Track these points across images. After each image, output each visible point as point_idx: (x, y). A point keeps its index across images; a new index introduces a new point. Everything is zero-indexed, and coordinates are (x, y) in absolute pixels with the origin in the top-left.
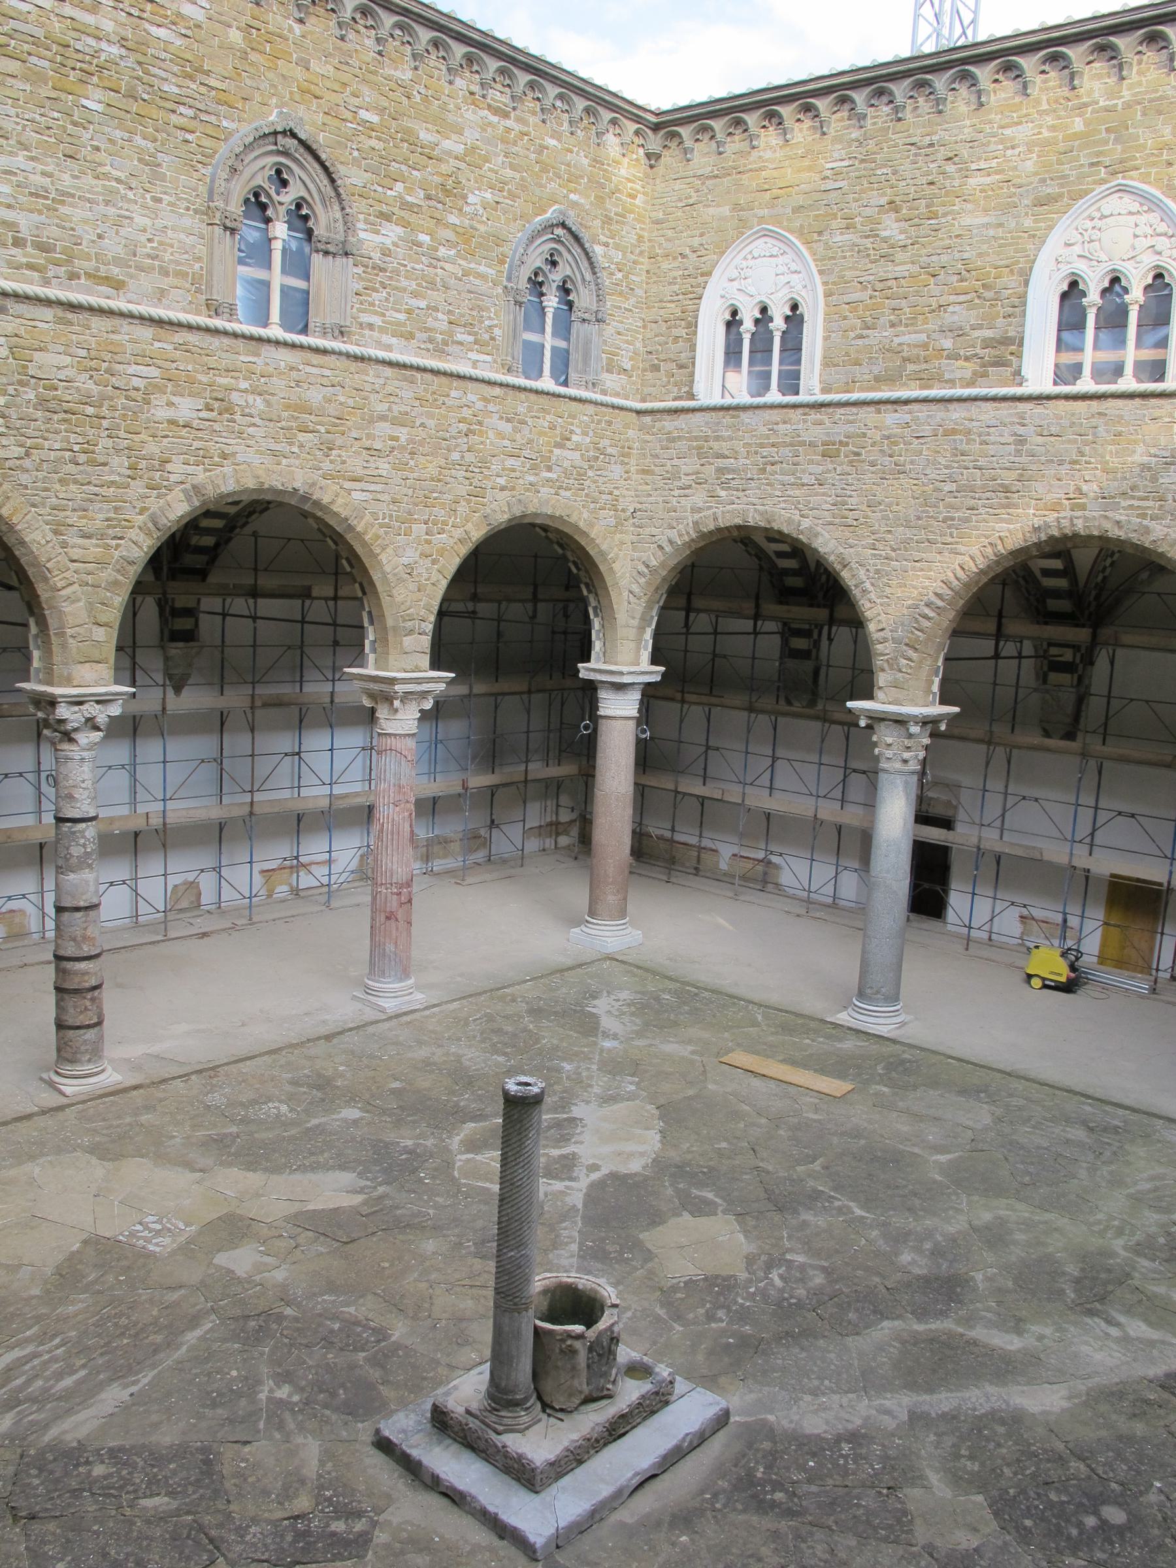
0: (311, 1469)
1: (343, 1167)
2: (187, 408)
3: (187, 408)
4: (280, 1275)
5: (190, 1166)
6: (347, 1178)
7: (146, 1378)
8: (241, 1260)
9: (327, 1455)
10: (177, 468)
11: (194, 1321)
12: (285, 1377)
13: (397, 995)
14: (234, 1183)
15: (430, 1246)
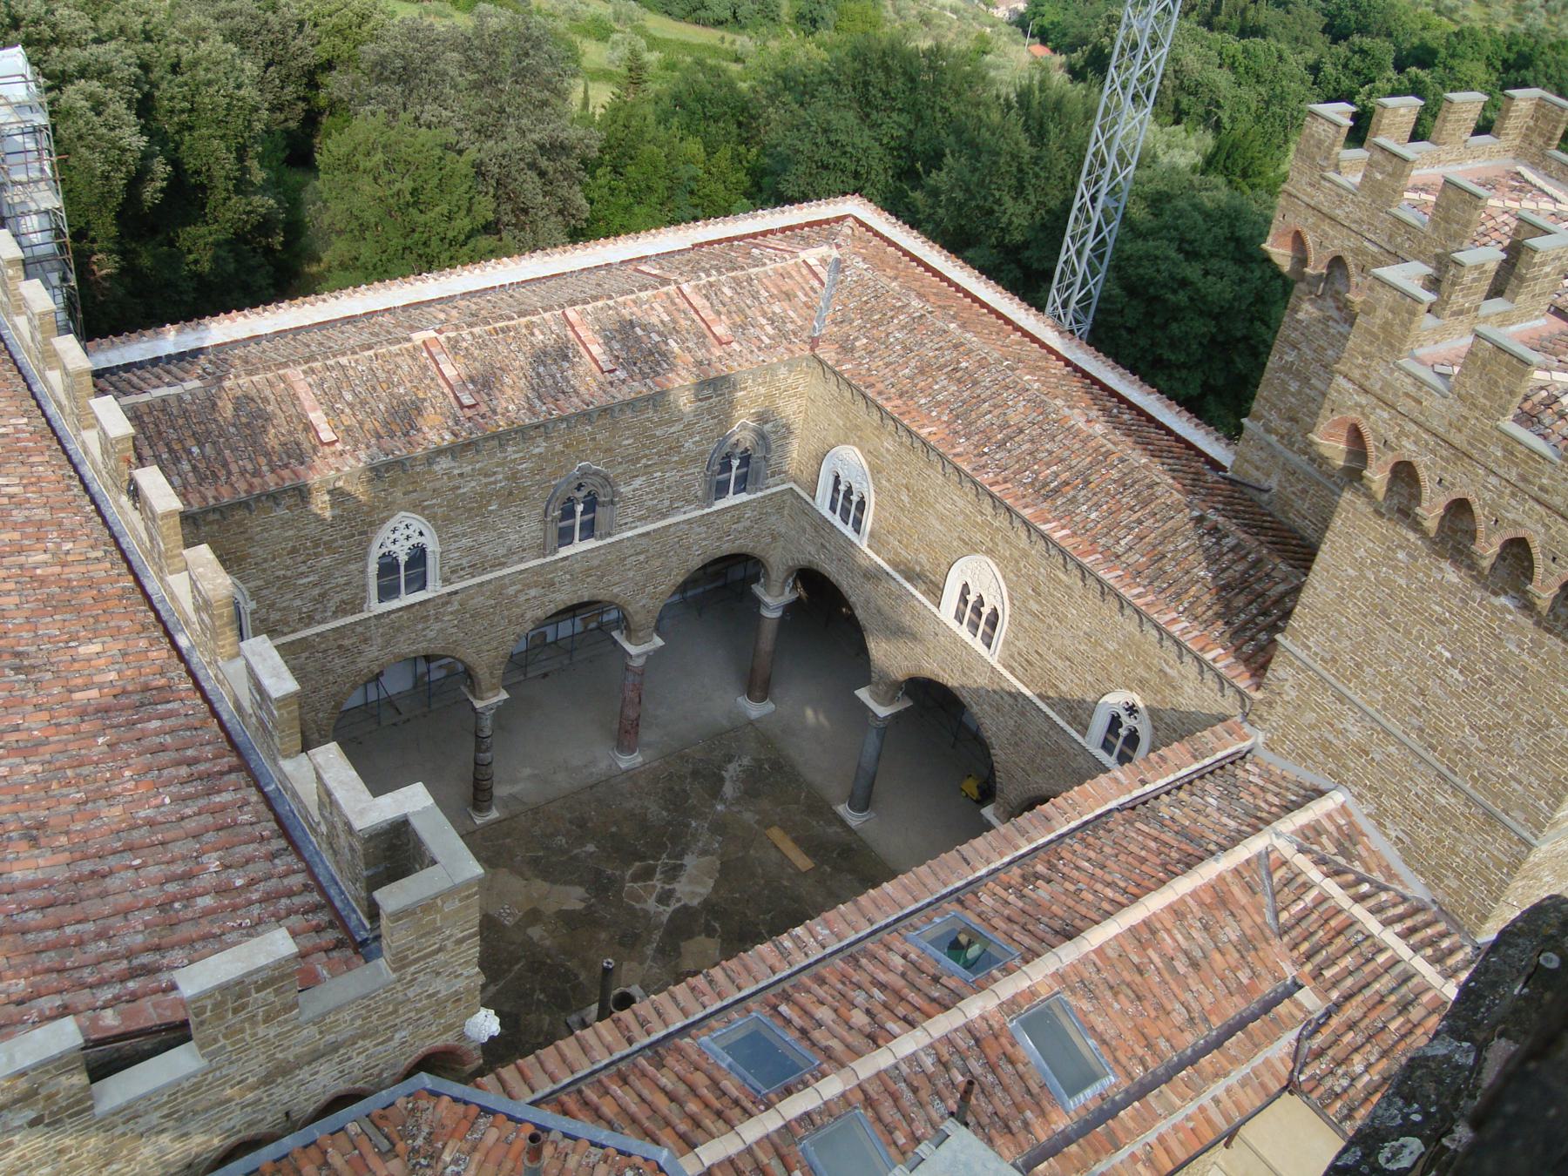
0: (546, 1027)
1: (581, 884)
2: (533, 592)
3: (533, 592)
4: (548, 943)
5: (522, 875)
6: (579, 891)
7: (502, 983)
8: (536, 932)
9: (551, 1023)
10: (528, 615)
11: (518, 960)
12: (543, 991)
13: (626, 762)
14: (540, 886)
15: (603, 936)
